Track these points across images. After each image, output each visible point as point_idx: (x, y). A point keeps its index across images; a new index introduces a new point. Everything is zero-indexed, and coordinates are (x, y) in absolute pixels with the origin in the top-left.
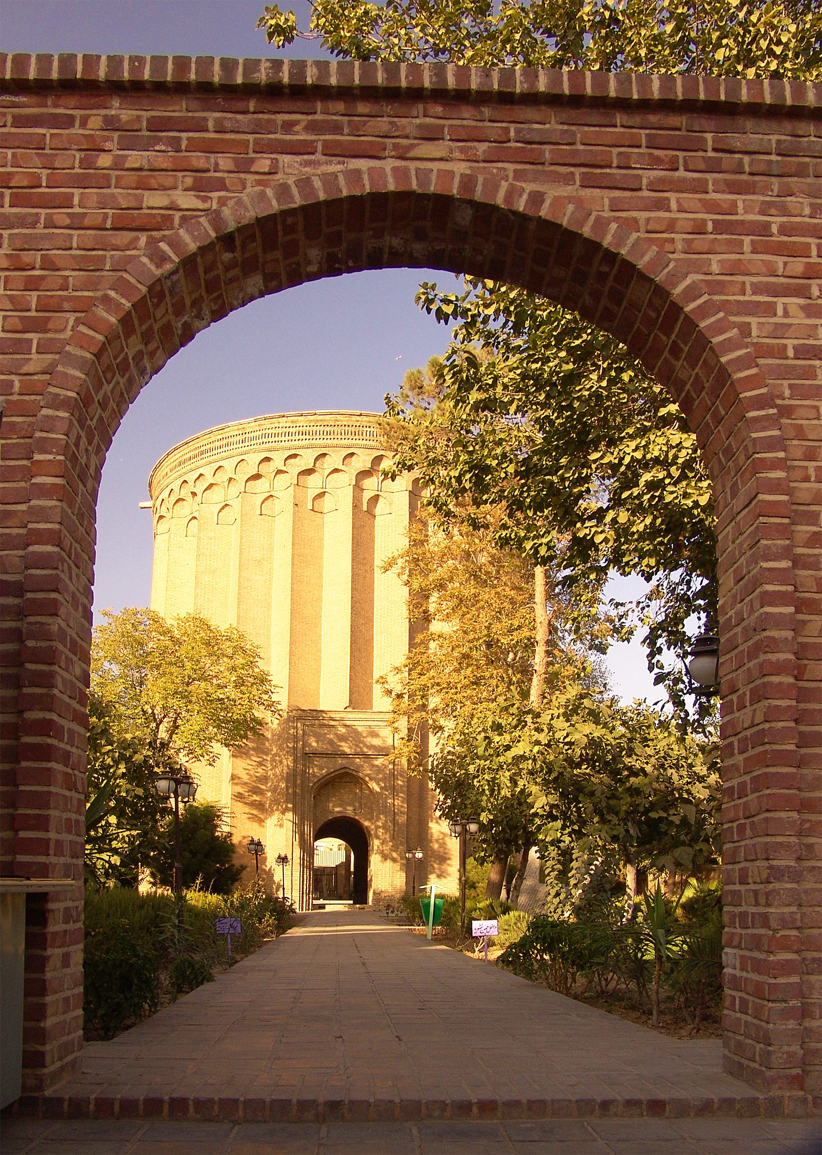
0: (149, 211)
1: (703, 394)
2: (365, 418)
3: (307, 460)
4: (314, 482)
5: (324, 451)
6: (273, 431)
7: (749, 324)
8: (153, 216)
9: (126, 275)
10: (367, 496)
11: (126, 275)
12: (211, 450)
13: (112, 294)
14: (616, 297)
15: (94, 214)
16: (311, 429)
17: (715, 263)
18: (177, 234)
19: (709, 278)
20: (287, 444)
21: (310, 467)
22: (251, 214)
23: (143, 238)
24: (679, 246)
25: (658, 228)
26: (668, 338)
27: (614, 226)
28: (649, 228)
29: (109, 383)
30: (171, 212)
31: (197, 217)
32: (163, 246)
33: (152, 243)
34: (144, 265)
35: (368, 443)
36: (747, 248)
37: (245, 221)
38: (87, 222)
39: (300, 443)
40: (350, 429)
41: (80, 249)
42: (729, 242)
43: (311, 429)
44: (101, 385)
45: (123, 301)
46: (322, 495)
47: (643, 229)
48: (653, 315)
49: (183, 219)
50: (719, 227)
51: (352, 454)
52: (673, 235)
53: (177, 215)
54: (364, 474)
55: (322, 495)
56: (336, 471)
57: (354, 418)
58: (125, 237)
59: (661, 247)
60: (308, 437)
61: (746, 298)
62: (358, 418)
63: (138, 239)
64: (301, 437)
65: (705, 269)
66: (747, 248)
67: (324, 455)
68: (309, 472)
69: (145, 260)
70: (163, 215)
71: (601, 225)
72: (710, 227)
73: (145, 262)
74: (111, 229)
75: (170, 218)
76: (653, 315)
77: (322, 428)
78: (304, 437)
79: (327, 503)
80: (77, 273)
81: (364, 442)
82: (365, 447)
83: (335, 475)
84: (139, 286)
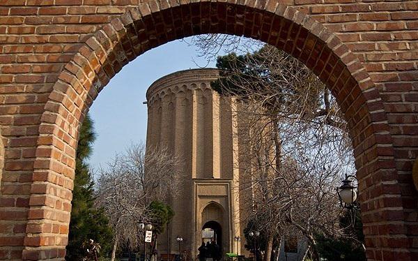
1: (343, 88)
14: (300, 44)
26: (325, 62)
44: (75, 96)
48: (318, 52)
76: (318, 52)
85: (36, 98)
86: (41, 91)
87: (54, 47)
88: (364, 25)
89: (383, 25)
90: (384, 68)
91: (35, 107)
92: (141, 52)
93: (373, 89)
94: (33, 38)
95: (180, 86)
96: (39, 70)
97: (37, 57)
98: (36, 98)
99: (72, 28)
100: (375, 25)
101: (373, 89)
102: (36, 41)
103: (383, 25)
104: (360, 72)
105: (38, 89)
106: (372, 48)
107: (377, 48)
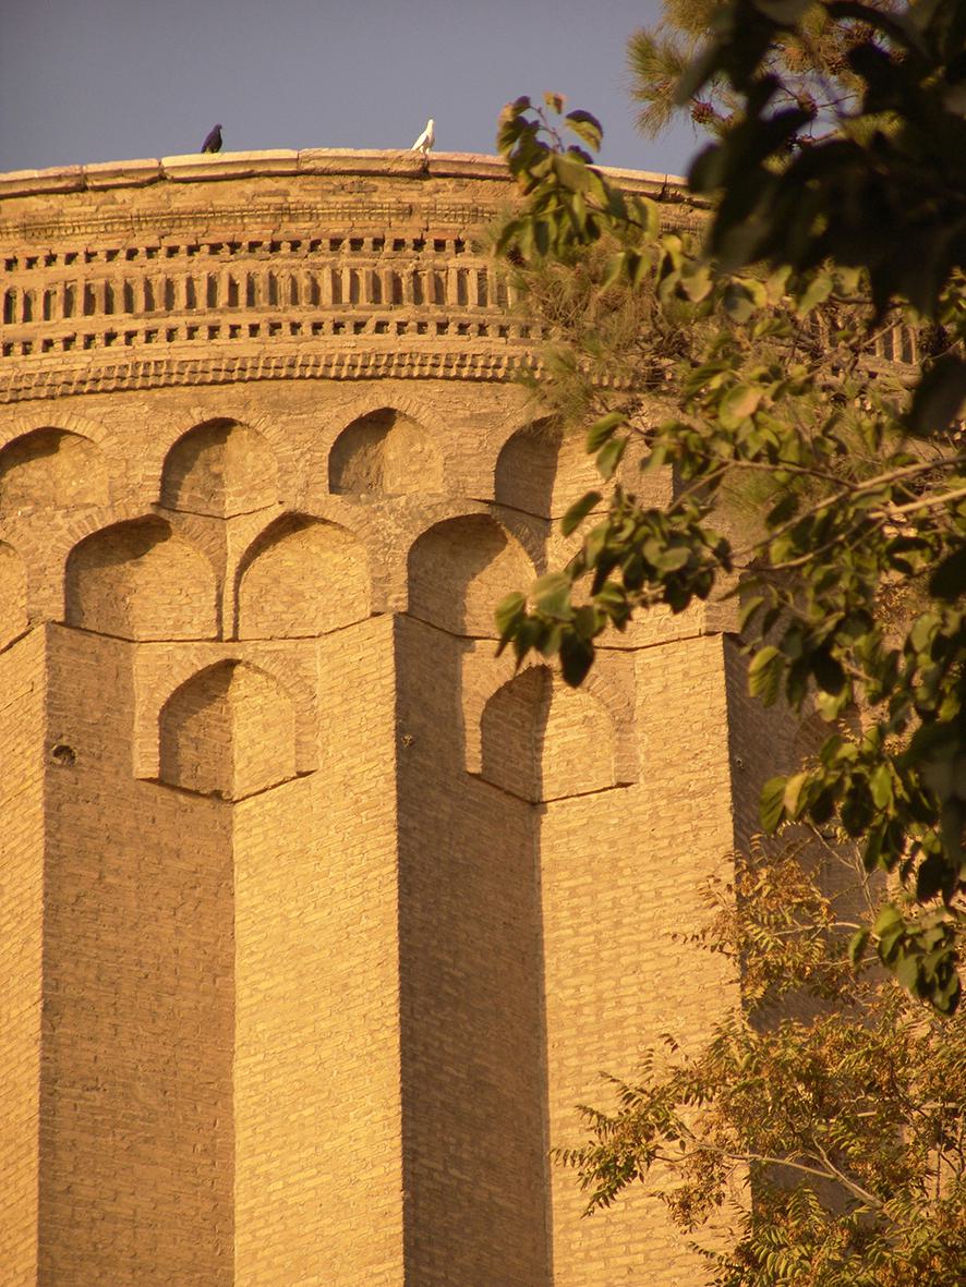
2: (450, 195)
3: (109, 468)
4: (168, 600)
5: (220, 403)
10: (485, 671)
16: (137, 270)
21: (141, 504)
35: (471, 345)
40: (365, 263)
43: (137, 270)
46: (212, 682)
51: (382, 420)
54: (455, 542)
55: (212, 682)
56: (292, 523)
57: (386, 195)
60: (121, 321)
62: (411, 195)
67: (219, 429)
68: (131, 538)
77: (203, 266)
78: (99, 323)
79: (252, 725)
81: (452, 342)
82: (457, 372)
83: (287, 553)
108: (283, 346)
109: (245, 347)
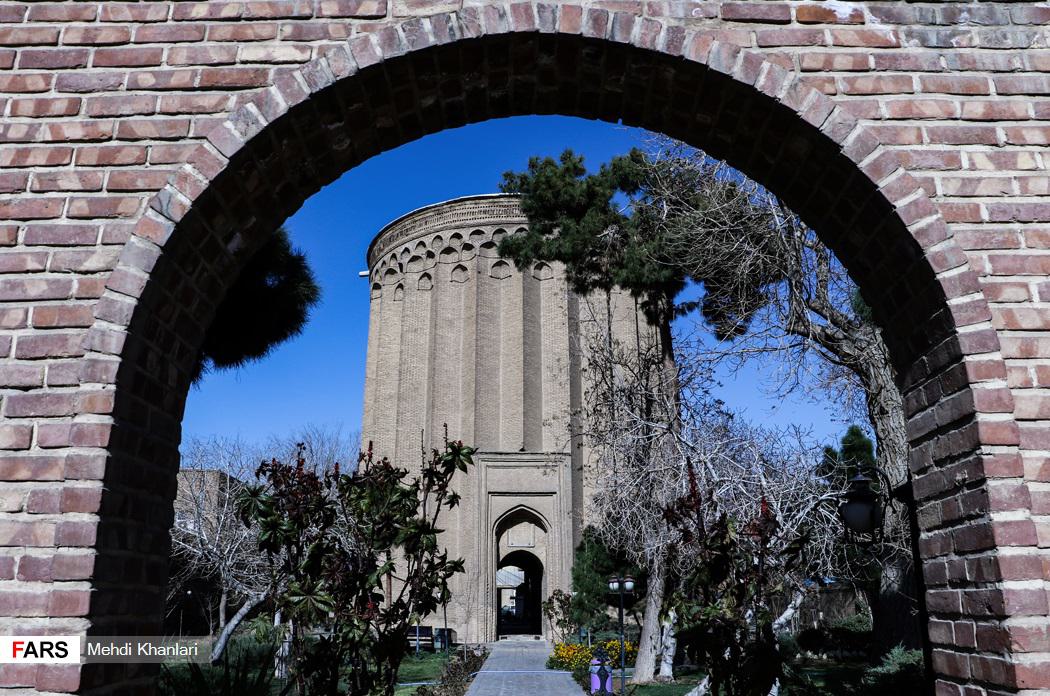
0: (242, 66)
6: (461, 211)
7: (933, 179)
8: (246, 71)
9: (206, 145)
11: (206, 145)
12: (413, 227)
13: (188, 168)
15: (182, 77)
17: (885, 106)
18: (268, 93)
19: (878, 124)
20: (472, 222)
22: (347, 68)
23: (233, 98)
24: (841, 86)
25: (814, 65)
27: (766, 65)
28: (805, 65)
29: (190, 274)
30: (266, 66)
31: (293, 70)
32: (251, 107)
33: (242, 102)
34: (229, 131)
36: (917, 86)
37: (344, 74)
38: (173, 82)
39: (482, 221)
41: (164, 114)
42: (895, 80)
45: (200, 177)
47: (797, 68)
49: (279, 72)
50: (883, 64)
52: (832, 74)
53: (272, 70)
58: (210, 99)
59: (821, 88)
61: (924, 147)
63: (227, 99)
64: (484, 216)
65: (873, 114)
66: (917, 86)
69: (229, 125)
70: (257, 70)
71: (752, 63)
72: (872, 63)
73: (233, 127)
74: (202, 89)
75: (265, 73)
80: (157, 142)
84: (220, 157)
85: (75, 286)
86: (88, 265)
87: (124, 152)
88: (931, 103)
89: (977, 107)
90: (985, 216)
91: (70, 310)
92: (354, 160)
93: (964, 269)
94: (73, 128)
95: (447, 235)
96: (86, 212)
97: (82, 177)
98: (75, 286)
99: (174, 100)
100: (957, 105)
101: (964, 269)
102: (78, 134)
103: (977, 107)
104: (930, 226)
105: (80, 262)
106: (952, 163)
107: (965, 164)
108: (509, 219)
109: (504, 219)
